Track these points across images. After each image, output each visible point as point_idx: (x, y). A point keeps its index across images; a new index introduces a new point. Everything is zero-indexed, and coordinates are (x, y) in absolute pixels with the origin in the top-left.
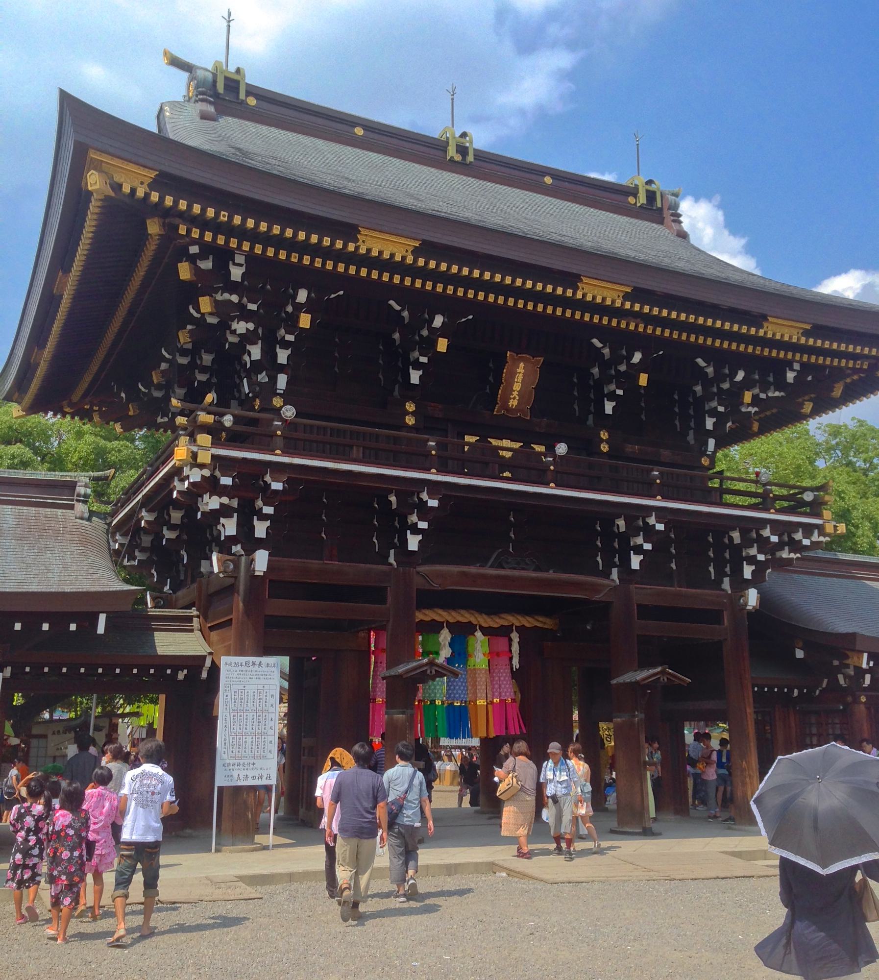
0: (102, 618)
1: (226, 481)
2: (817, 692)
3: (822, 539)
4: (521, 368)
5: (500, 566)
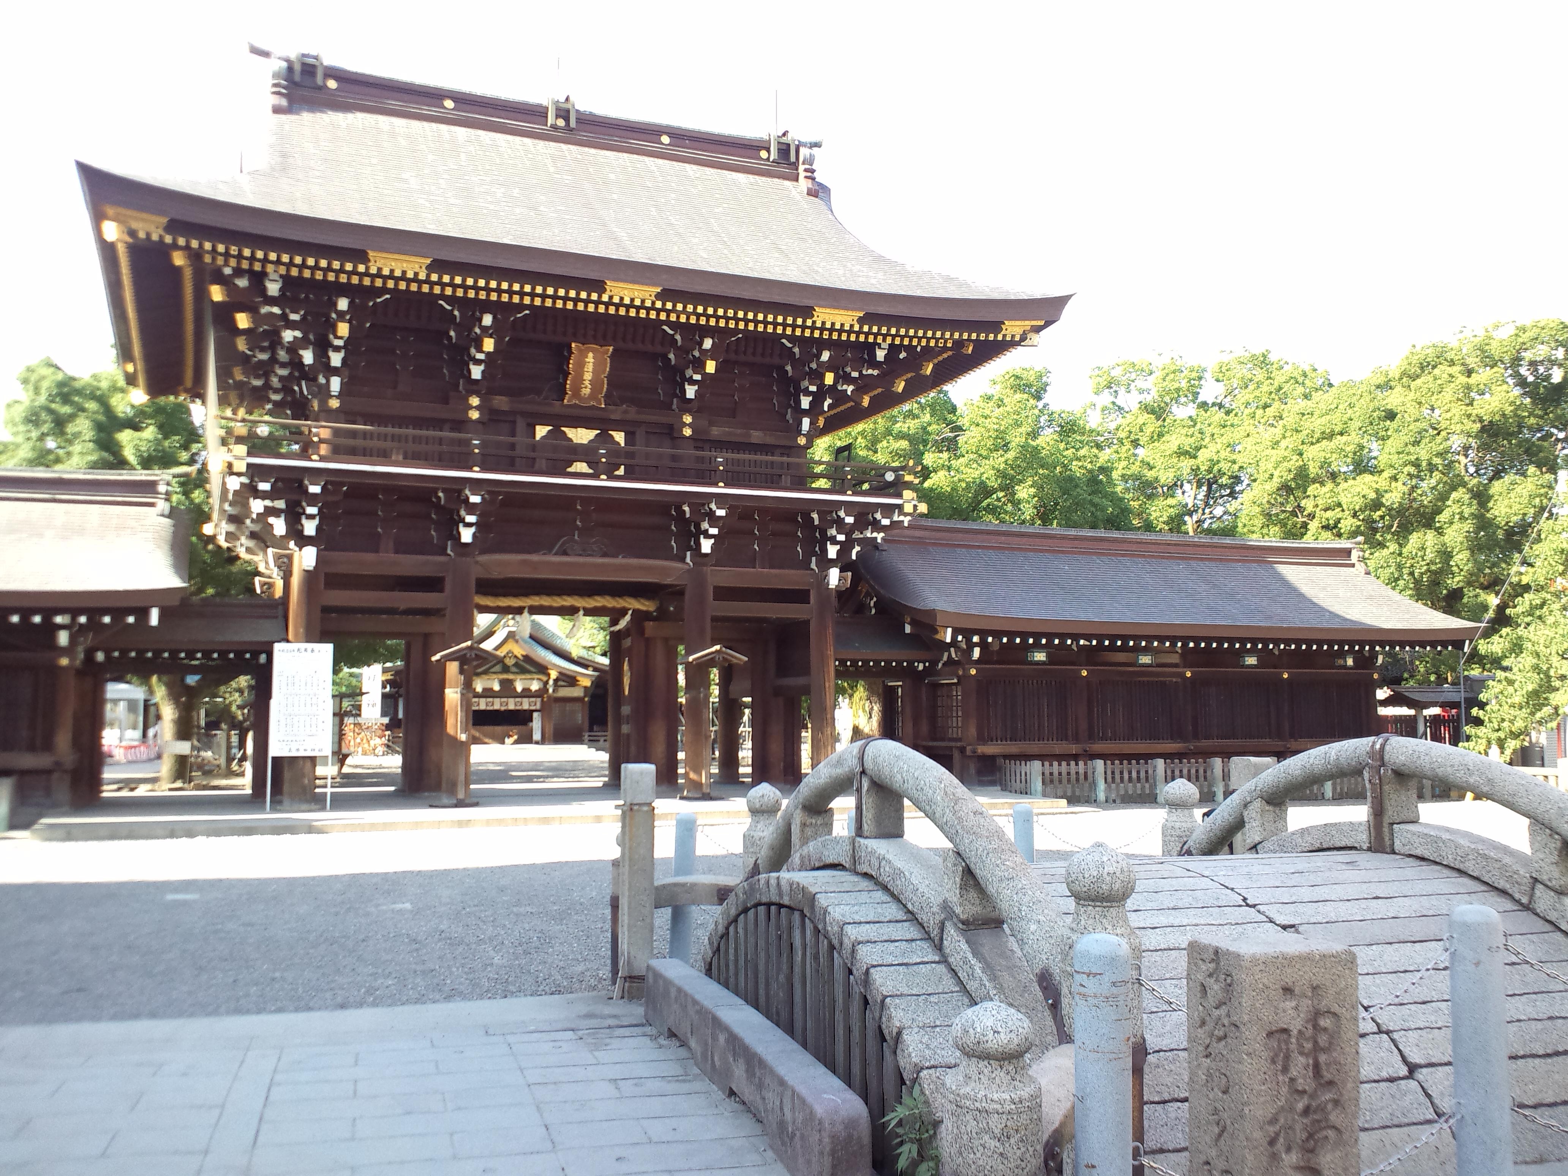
1: (264, 486)
2: (940, 665)
3: (902, 518)
4: (590, 358)
5: (565, 553)
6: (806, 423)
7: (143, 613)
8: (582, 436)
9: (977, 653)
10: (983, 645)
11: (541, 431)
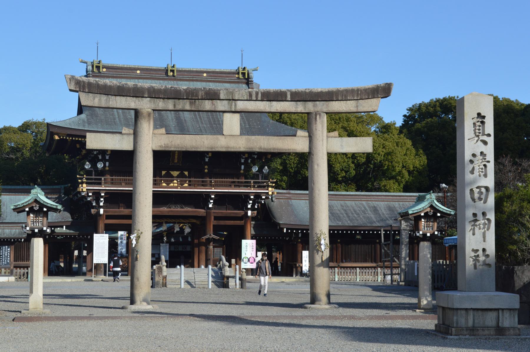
0: (64, 227)
1: (90, 194)
6: (243, 167)
8: (175, 173)
9: (300, 235)
10: (302, 232)
11: (164, 173)
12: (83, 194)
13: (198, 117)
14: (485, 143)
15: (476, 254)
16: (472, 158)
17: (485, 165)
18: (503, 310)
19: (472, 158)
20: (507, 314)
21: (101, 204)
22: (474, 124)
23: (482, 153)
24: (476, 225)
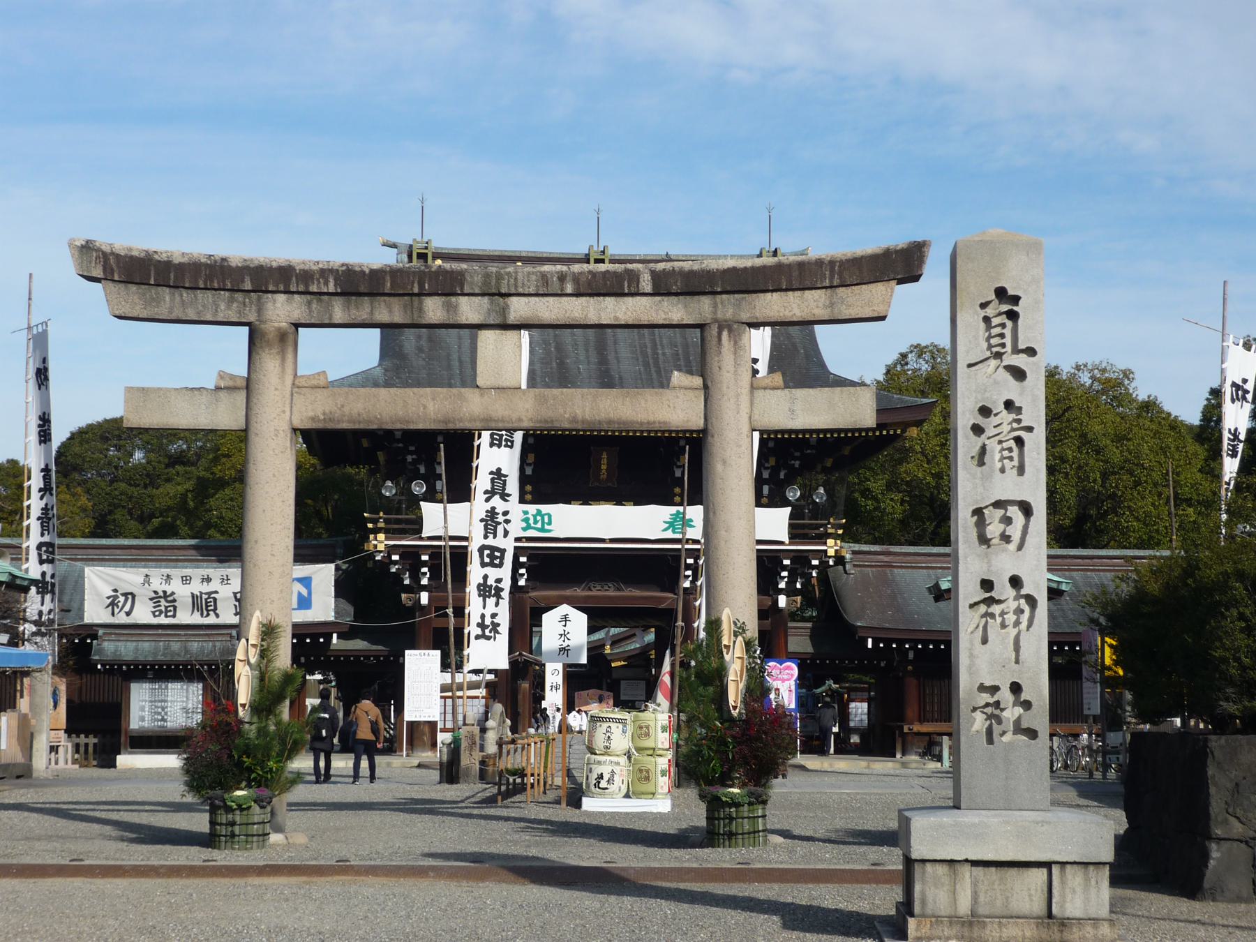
1: (395, 558)
7: (328, 637)
9: (911, 655)
10: (914, 648)
12: (379, 558)
13: (653, 370)
14: (1019, 374)
15: (991, 700)
16: (980, 420)
17: (1019, 441)
18: (1063, 864)
19: (980, 420)
20: (1075, 878)
21: (424, 581)
22: (987, 320)
23: (1009, 405)
24: (992, 616)
